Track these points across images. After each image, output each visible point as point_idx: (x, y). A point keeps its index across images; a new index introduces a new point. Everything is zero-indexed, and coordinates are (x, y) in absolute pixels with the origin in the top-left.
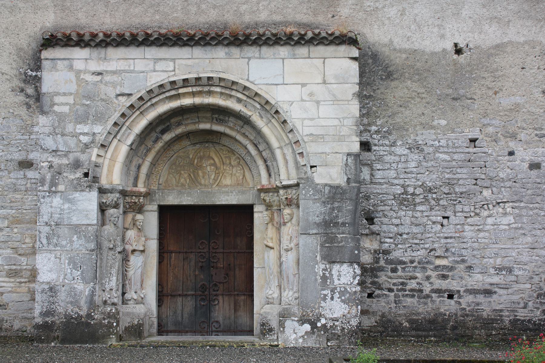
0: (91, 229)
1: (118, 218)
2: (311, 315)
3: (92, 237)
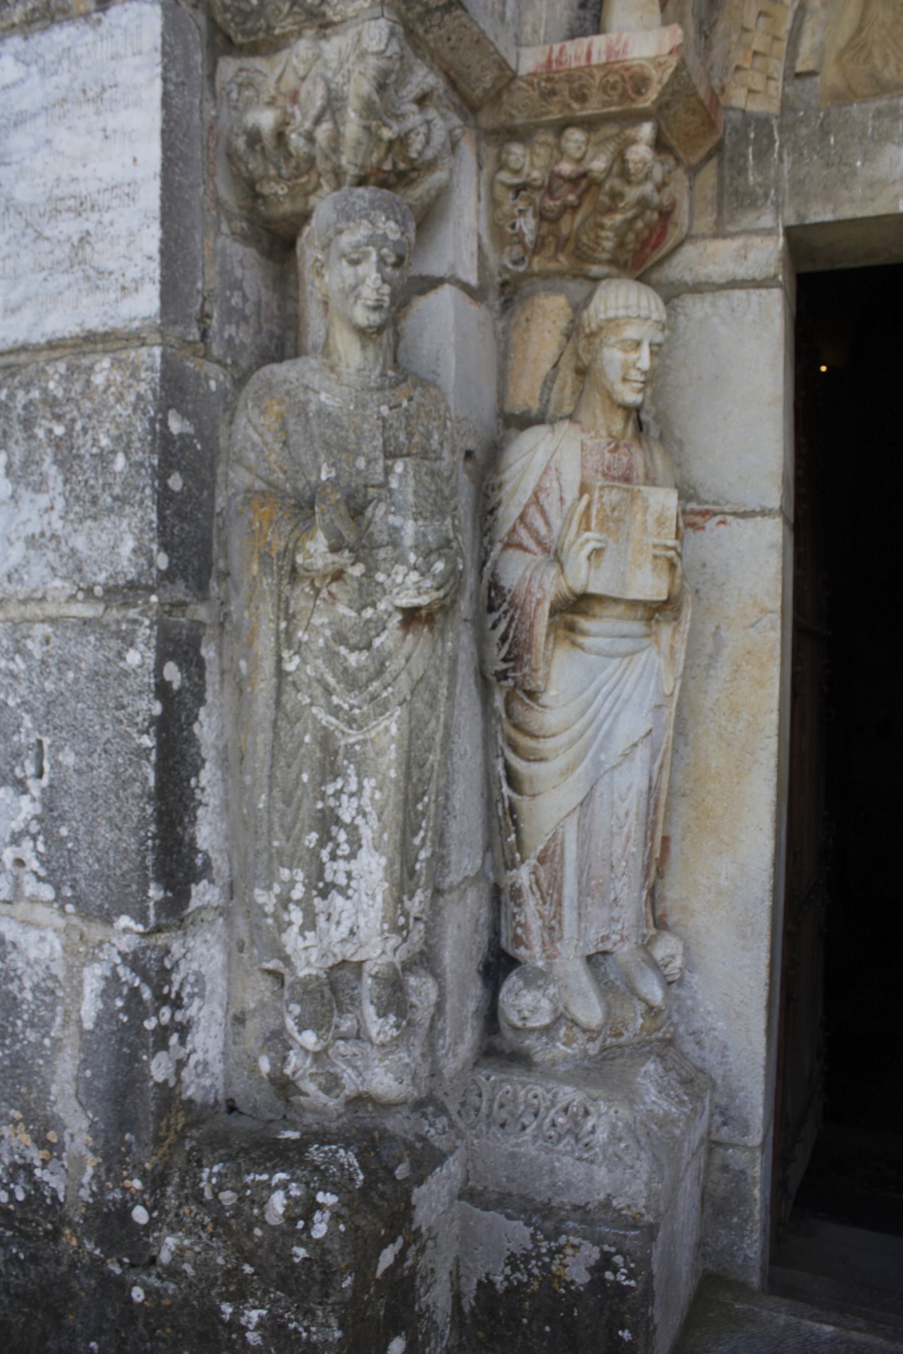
0: (118, 376)
3: (120, 463)
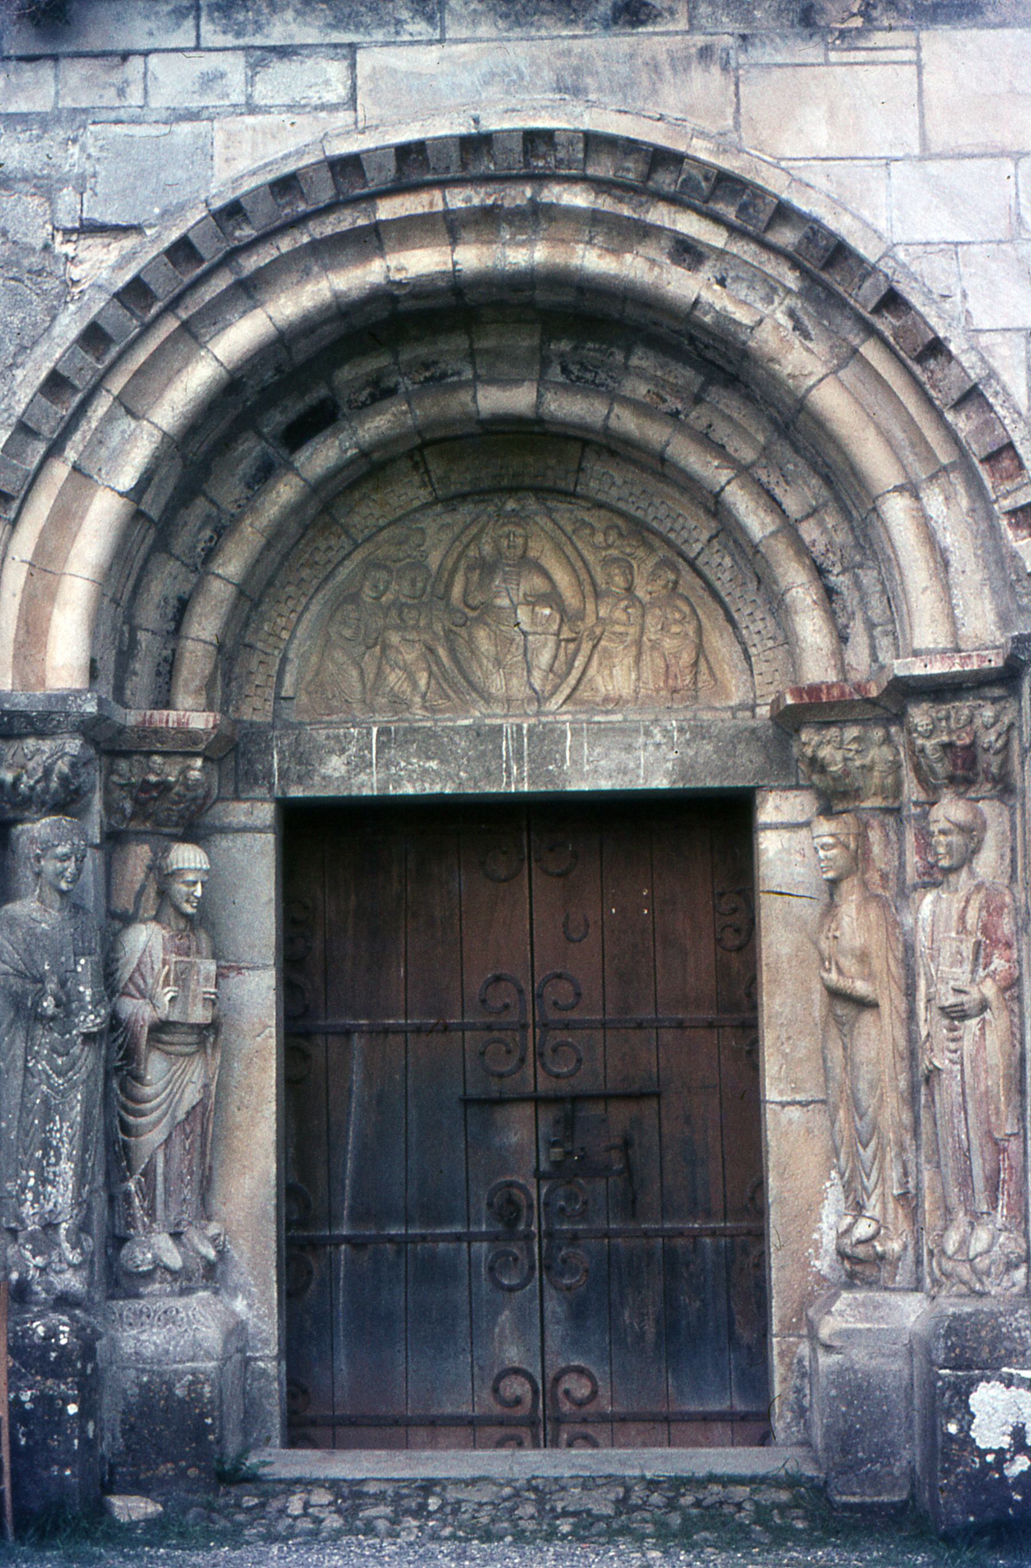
1: (80, 860)
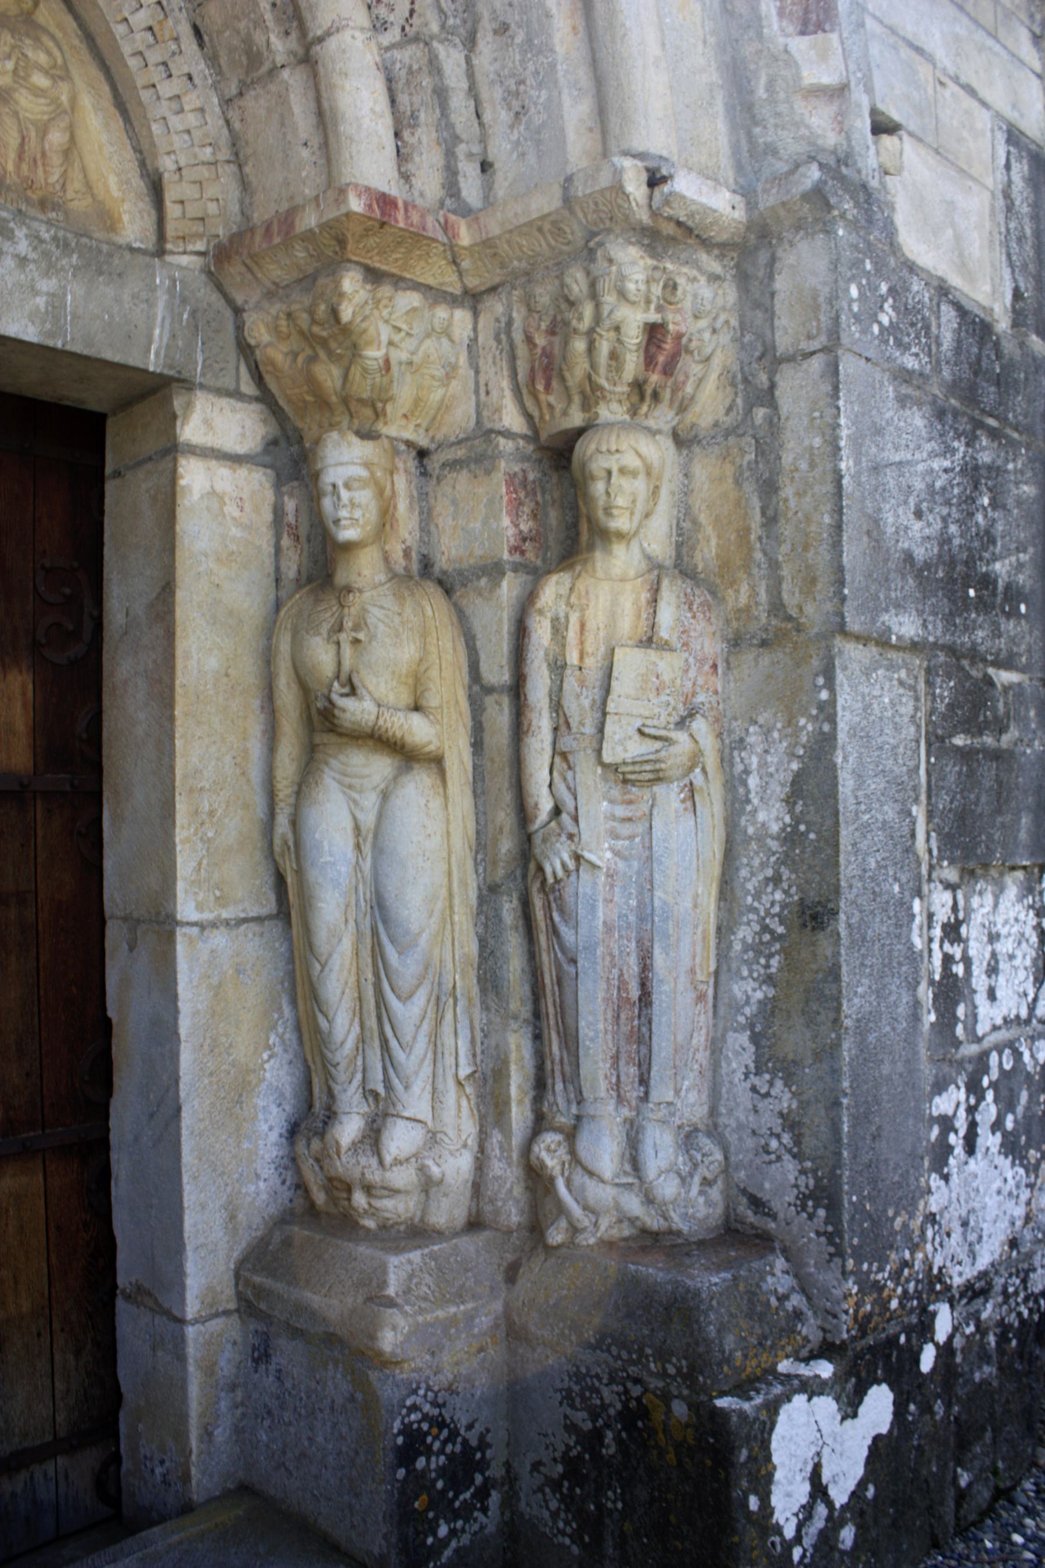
2: (894, 1304)
